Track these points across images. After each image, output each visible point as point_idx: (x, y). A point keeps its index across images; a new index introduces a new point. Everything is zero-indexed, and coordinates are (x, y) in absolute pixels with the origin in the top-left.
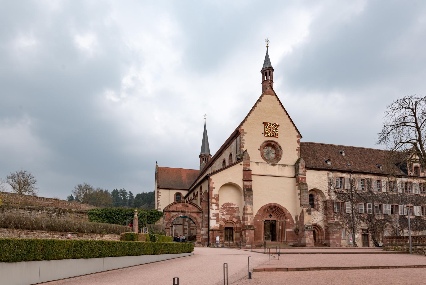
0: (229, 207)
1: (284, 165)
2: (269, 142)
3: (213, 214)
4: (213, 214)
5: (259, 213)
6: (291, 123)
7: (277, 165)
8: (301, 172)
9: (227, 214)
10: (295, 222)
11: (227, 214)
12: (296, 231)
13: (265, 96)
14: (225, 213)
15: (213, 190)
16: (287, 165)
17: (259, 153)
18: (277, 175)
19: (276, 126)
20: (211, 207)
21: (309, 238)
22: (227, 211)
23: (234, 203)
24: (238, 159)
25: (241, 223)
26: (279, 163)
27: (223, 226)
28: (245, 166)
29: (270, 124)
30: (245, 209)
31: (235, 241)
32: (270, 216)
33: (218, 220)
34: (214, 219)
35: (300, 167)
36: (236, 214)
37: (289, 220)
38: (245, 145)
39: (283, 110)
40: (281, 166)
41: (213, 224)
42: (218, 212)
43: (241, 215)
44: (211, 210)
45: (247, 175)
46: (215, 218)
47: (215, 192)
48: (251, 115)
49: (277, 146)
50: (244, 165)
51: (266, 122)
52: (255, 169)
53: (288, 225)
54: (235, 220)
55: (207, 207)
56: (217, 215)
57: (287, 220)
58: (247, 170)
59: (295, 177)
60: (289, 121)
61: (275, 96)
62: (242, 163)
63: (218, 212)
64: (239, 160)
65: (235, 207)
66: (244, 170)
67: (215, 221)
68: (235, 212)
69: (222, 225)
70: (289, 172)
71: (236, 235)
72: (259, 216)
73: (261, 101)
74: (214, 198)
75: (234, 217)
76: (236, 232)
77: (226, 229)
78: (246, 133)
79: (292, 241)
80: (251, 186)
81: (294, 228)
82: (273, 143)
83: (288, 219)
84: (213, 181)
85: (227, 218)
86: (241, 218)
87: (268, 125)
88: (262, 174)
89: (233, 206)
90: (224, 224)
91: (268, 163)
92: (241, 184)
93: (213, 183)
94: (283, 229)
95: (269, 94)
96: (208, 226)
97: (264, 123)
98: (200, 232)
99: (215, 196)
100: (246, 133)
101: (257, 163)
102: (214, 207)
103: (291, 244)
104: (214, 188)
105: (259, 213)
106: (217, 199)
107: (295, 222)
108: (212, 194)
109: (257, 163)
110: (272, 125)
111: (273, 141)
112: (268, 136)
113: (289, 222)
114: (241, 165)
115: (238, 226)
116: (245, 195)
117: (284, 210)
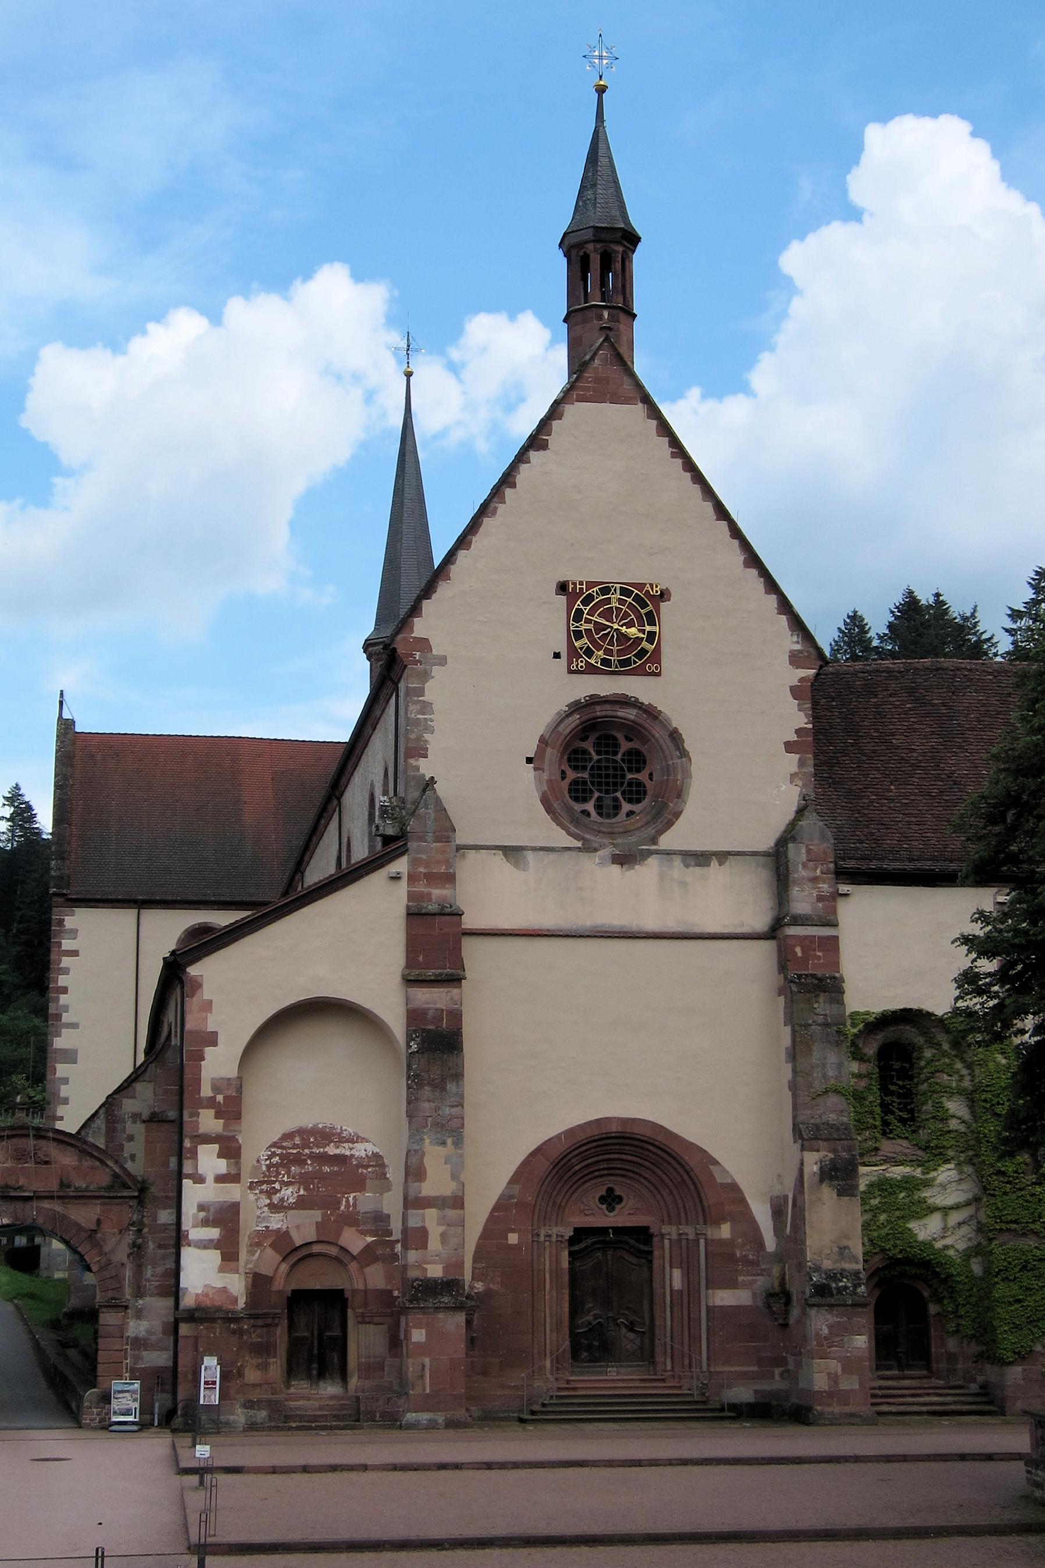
0: (313, 1157)
1: (700, 858)
2: (599, 711)
3: (201, 1207)
4: (201, 1207)
5: (517, 1189)
6: (754, 572)
7: (653, 862)
8: (802, 901)
9: (301, 1204)
10: (770, 1243)
11: (301, 1204)
12: (779, 1298)
13: (573, 411)
14: (289, 1194)
15: (209, 1051)
16: (722, 856)
17: (527, 785)
18: (651, 924)
19: (646, 603)
20: (187, 1168)
21: (840, 1353)
22: (304, 1180)
23: (350, 1129)
24: (387, 840)
25: (395, 1257)
26: (668, 841)
27: (279, 1284)
28: (421, 888)
29: (605, 591)
30: (415, 1172)
31: (353, 1382)
32: (611, 1200)
33: (229, 1254)
34: (205, 1245)
35: (800, 872)
36: (365, 1201)
37: (725, 1231)
38: (435, 742)
39: (696, 490)
40: (677, 861)
41: (201, 1273)
42: (233, 1192)
43: (391, 1203)
44: (187, 1183)
45: (436, 945)
46: (214, 1233)
47: (218, 1064)
48: (478, 541)
49: (658, 733)
50: (412, 878)
51: (574, 575)
52: (490, 894)
53: (726, 1265)
54: (355, 1241)
55: (173, 1161)
56: (225, 1218)
57: (712, 1233)
58: (432, 908)
59: (773, 933)
60: (739, 557)
61: (639, 408)
62: (401, 865)
63: (233, 1192)
64: (391, 846)
65: (360, 1150)
66: (415, 915)
67: (214, 1256)
68: (359, 1184)
69: (270, 1279)
70: (733, 900)
71: (363, 1341)
72: (521, 1205)
73: (544, 446)
74: (211, 1103)
75: (351, 1219)
76: (363, 1320)
77: (299, 1299)
78: (442, 661)
79: (746, 1375)
80: (456, 1016)
81: (761, 1283)
82: (631, 714)
83: (718, 1222)
84: (207, 992)
85: (303, 1226)
86: (396, 1226)
87: (589, 599)
88: (547, 922)
89: (344, 1150)
90: (284, 1267)
91: (588, 848)
92: (390, 1005)
93: (208, 1006)
94: (691, 1293)
95: (604, 394)
96: (172, 1287)
97: (562, 588)
98: (121, 1328)
99: (216, 1088)
100: (442, 661)
101: (512, 853)
102: (209, 1161)
103: (743, 1394)
104: (212, 1039)
105: (517, 1189)
106: (231, 1109)
107: (770, 1243)
108: (198, 1081)
109: (512, 853)
110: (615, 597)
111: (623, 701)
112: (591, 670)
113: (730, 1243)
114: (396, 878)
115: (376, 1277)
116: (415, 1081)
117: (693, 1162)
